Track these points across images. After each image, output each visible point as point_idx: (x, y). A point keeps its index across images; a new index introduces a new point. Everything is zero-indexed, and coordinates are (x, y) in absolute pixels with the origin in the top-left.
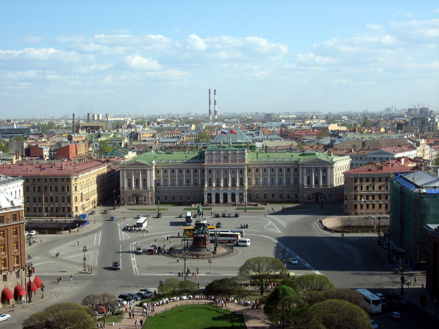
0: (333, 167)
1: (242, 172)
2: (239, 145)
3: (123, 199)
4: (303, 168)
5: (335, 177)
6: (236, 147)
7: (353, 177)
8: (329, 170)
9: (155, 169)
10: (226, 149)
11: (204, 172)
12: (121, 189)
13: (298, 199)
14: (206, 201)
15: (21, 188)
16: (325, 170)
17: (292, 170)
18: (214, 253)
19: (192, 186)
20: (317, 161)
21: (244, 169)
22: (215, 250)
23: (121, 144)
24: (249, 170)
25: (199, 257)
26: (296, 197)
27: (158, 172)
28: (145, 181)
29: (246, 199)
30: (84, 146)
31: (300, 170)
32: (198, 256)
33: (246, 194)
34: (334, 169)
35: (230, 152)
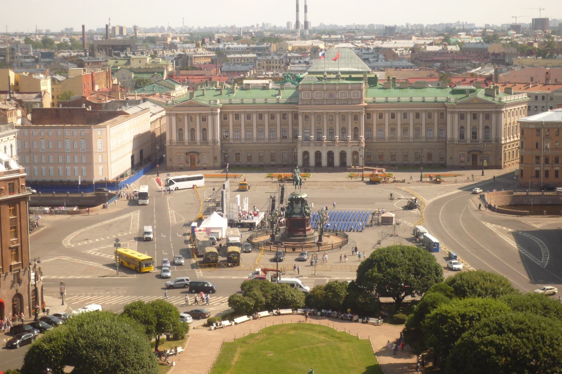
0: (502, 112)
1: (356, 118)
2: (353, 76)
3: (170, 160)
4: (452, 113)
5: (503, 127)
6: (347, 79)
7: (533, 126)
8: (494, 117)
9: (221, 112)
10: (332, 82)
11: (298, 119)
12: (168, 144)
13: (443, 162)
14: (300, 162)
15: (14, 142)
16: (487, 116)
17: (436, 116)
18: (319, 244)
19: (279, 141)
20: (476, 101)
21: (360, 113)
22: (320, 239)
23: (162, 73)
24: (368, 115)
25: (296, 251)
26: (442, 159)
27: (225, 118)
28: (204, 131)
29: (361, 161)
30: (105, 76)
31: (449, 116)
32: (294, 249)
33: (362, 153)
34: (503, 115)
35: (337, 87)
